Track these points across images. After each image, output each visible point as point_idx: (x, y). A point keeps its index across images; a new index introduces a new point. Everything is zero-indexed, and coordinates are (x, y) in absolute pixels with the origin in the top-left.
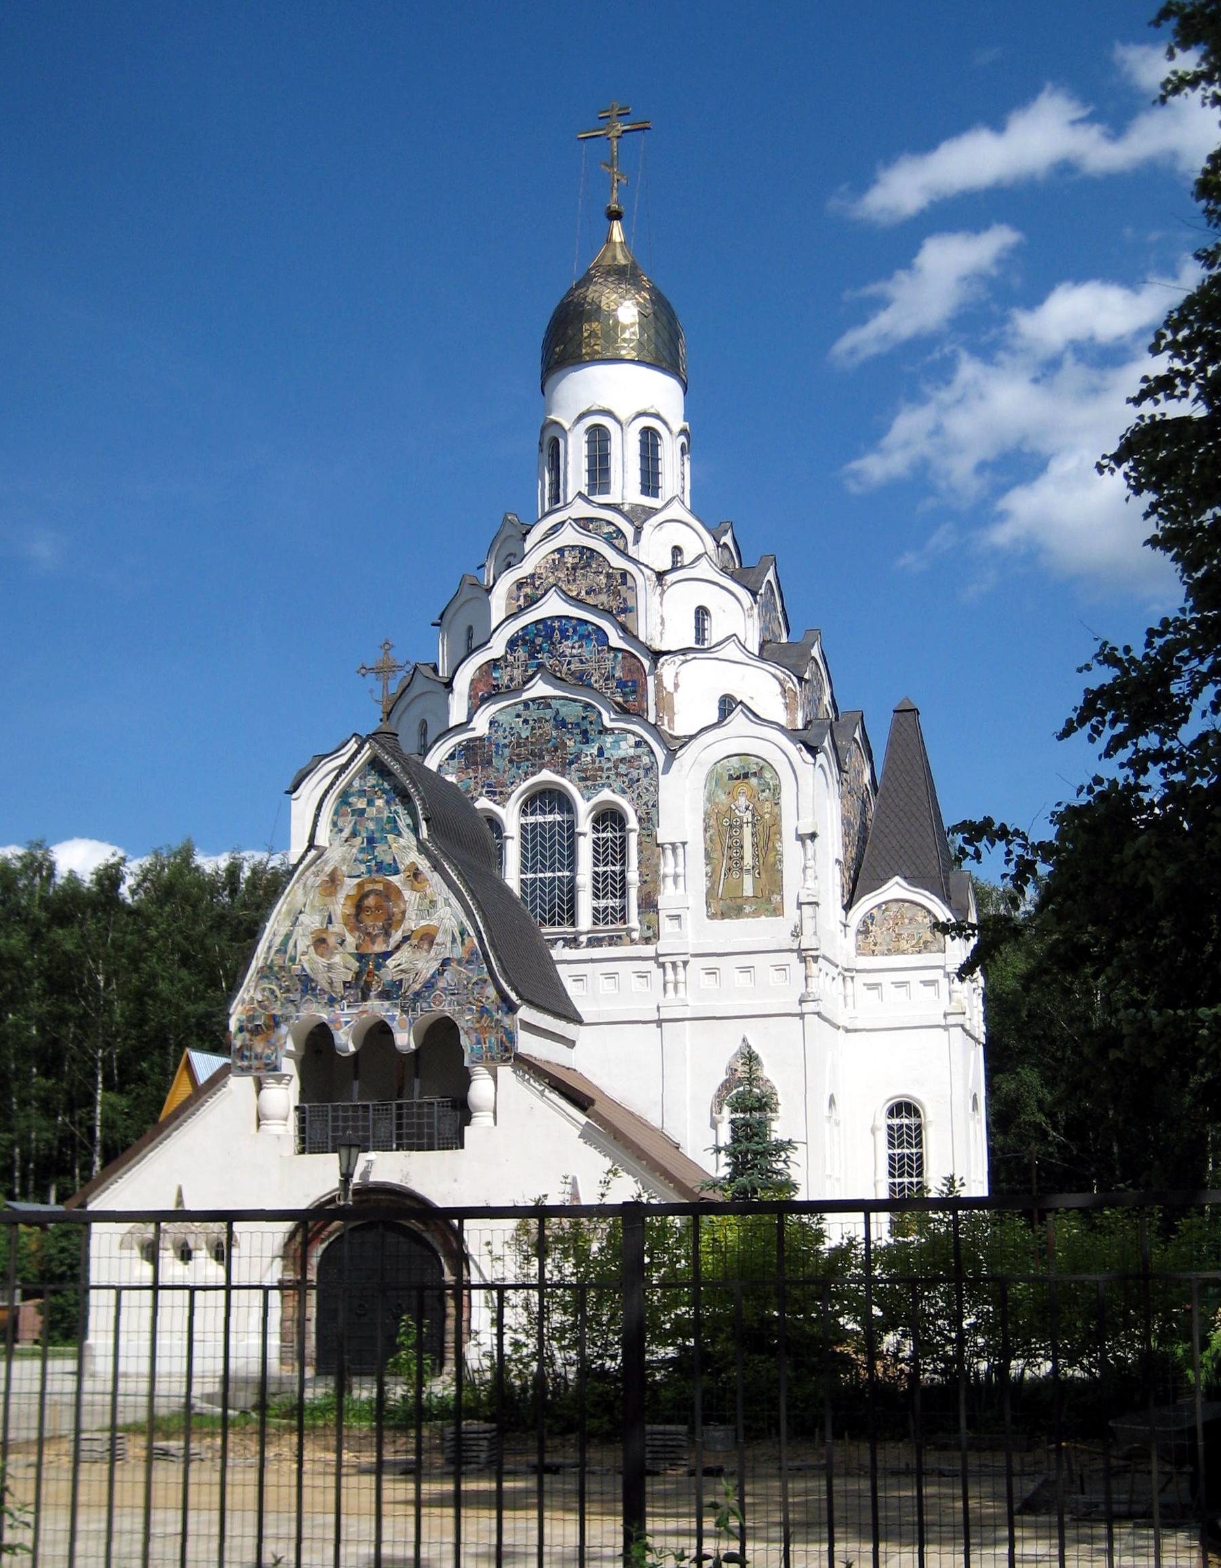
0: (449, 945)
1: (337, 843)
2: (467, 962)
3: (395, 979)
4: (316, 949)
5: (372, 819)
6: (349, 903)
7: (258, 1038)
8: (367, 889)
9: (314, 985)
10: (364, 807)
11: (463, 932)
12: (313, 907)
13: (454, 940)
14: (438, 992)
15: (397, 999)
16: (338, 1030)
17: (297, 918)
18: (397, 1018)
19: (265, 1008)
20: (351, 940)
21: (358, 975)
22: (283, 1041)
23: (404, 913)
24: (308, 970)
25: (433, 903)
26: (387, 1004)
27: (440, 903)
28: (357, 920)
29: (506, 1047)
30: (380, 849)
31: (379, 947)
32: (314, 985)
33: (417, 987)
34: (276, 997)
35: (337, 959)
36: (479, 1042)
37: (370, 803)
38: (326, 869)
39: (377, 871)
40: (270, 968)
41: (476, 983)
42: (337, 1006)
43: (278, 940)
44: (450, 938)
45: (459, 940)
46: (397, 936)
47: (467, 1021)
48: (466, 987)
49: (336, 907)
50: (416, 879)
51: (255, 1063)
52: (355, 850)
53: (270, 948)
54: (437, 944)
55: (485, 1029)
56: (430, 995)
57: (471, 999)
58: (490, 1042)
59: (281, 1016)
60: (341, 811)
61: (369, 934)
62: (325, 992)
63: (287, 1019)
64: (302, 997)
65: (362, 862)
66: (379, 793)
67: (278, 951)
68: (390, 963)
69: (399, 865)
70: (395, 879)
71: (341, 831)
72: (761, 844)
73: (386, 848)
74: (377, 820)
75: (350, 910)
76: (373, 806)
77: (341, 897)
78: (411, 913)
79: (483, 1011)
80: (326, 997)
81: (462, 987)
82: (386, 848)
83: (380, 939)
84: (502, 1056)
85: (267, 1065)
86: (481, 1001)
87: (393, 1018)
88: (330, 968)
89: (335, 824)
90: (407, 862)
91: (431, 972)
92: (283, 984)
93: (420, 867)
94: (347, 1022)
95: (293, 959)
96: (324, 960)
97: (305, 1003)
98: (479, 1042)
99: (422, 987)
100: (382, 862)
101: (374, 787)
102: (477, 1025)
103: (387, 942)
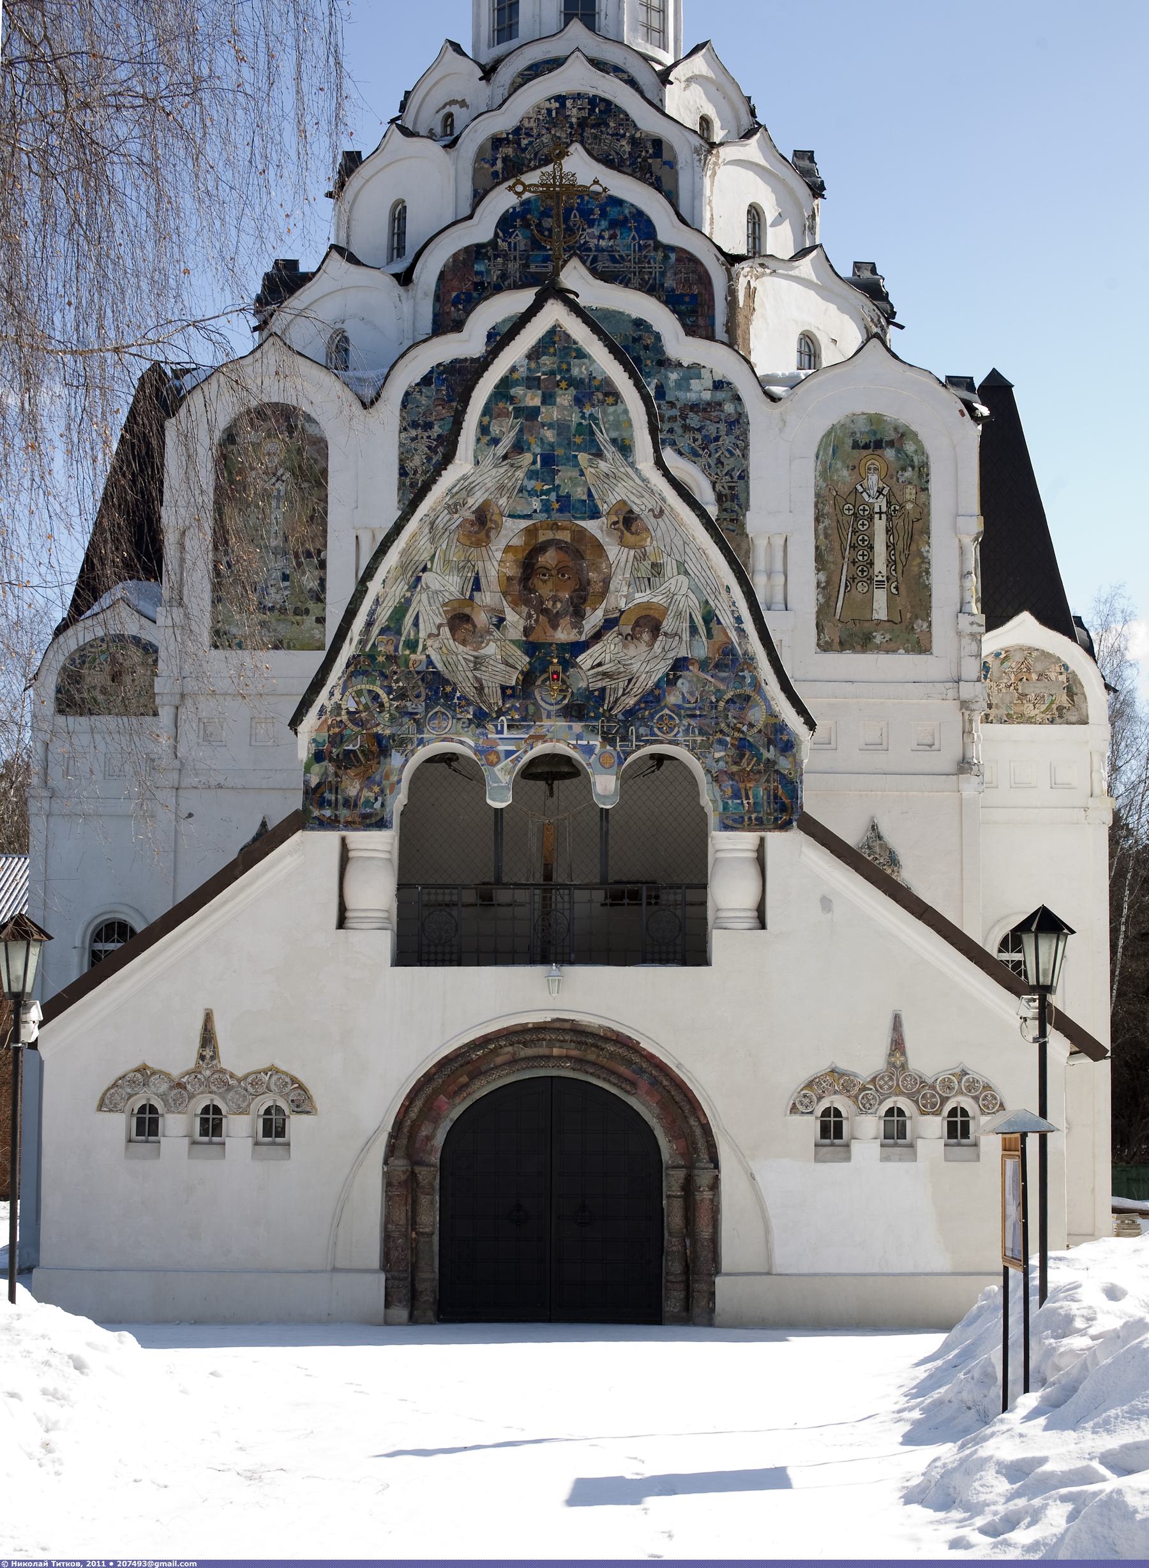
0: (686, 636)
1: (488, 462)
2: (717, 666)
4: (453, 630)
5: (551, 426)
6: (510, 556)
7: (351, 773)
8: (541, 539)
9: (449, 689)
10: (537, 402)
11: (710, 617)
12: (447, 562)
13: (694, 630)
14: (666, 711)
15: (596, 718)
16: (493, 765)
17: (419, 579)
19: (361, 724)
20: (514, 619)
21: (528, 678)
22: (394, 779)
23: (606, 582)
24: (440, 666)
25: (657, 569)
26: (578, 727)
27: (670, 568)
28: (525, 588)
29: (783, 804)
30: (565, 476)
31: (564, 634)
32: (449, 689)
33: (631, 701)
34: (382, 705)
35: (490, 649)
36: (736, 795)
37: (548, 399)
38: (471, 501)
39: (560, 510)
40: (372, 657)
41: (730, 701)
42: (490, 726)
43: (384, 616)
44: (686, 625)
45: (702, 629)
46: (594, 619)
47: (717, 761)
48: (714, 706)
49: (488, 565)
50: (628, 528)
51: (344, 813)
52: (520, 474)
53: (369, 624)
54: (666, 634)
55: (744, 776)
56: (652, 716)
58: (755, 796)
59: (392, 736)
60: (496, 411)
61: (545, 612)
64: (427, 711)
65: (533, 493)
66: (563, 384)
67: (382, 632)
68: (585, 660)
69: (599, 502)
70: (591, 526)
71: (495, 441)
72: (900, 546)
73: (576, 474)
74: (561, 427)
75: (512, 570)
76: (554, 404)
77: (497, 549)
78: (619, 583)
79: (743, 747)
80: (471, 710)
82: (576, 474)
83: (565, 621)
84: (776, 819)
86: (740, 731)
87: (589, 750)
88: (478, 663)
89: (484, 429)
90: (613, 499)
91: (655, 678)
93: (636, 509)
94: (509, 753)
95: (412, 645)
96: (467, 649)
97: (429, 721)
98: (736, 795)
99: (637, 703)
100: (568, 496)
101: (552, 373)
102: (735, 768)
103: (578, 625)
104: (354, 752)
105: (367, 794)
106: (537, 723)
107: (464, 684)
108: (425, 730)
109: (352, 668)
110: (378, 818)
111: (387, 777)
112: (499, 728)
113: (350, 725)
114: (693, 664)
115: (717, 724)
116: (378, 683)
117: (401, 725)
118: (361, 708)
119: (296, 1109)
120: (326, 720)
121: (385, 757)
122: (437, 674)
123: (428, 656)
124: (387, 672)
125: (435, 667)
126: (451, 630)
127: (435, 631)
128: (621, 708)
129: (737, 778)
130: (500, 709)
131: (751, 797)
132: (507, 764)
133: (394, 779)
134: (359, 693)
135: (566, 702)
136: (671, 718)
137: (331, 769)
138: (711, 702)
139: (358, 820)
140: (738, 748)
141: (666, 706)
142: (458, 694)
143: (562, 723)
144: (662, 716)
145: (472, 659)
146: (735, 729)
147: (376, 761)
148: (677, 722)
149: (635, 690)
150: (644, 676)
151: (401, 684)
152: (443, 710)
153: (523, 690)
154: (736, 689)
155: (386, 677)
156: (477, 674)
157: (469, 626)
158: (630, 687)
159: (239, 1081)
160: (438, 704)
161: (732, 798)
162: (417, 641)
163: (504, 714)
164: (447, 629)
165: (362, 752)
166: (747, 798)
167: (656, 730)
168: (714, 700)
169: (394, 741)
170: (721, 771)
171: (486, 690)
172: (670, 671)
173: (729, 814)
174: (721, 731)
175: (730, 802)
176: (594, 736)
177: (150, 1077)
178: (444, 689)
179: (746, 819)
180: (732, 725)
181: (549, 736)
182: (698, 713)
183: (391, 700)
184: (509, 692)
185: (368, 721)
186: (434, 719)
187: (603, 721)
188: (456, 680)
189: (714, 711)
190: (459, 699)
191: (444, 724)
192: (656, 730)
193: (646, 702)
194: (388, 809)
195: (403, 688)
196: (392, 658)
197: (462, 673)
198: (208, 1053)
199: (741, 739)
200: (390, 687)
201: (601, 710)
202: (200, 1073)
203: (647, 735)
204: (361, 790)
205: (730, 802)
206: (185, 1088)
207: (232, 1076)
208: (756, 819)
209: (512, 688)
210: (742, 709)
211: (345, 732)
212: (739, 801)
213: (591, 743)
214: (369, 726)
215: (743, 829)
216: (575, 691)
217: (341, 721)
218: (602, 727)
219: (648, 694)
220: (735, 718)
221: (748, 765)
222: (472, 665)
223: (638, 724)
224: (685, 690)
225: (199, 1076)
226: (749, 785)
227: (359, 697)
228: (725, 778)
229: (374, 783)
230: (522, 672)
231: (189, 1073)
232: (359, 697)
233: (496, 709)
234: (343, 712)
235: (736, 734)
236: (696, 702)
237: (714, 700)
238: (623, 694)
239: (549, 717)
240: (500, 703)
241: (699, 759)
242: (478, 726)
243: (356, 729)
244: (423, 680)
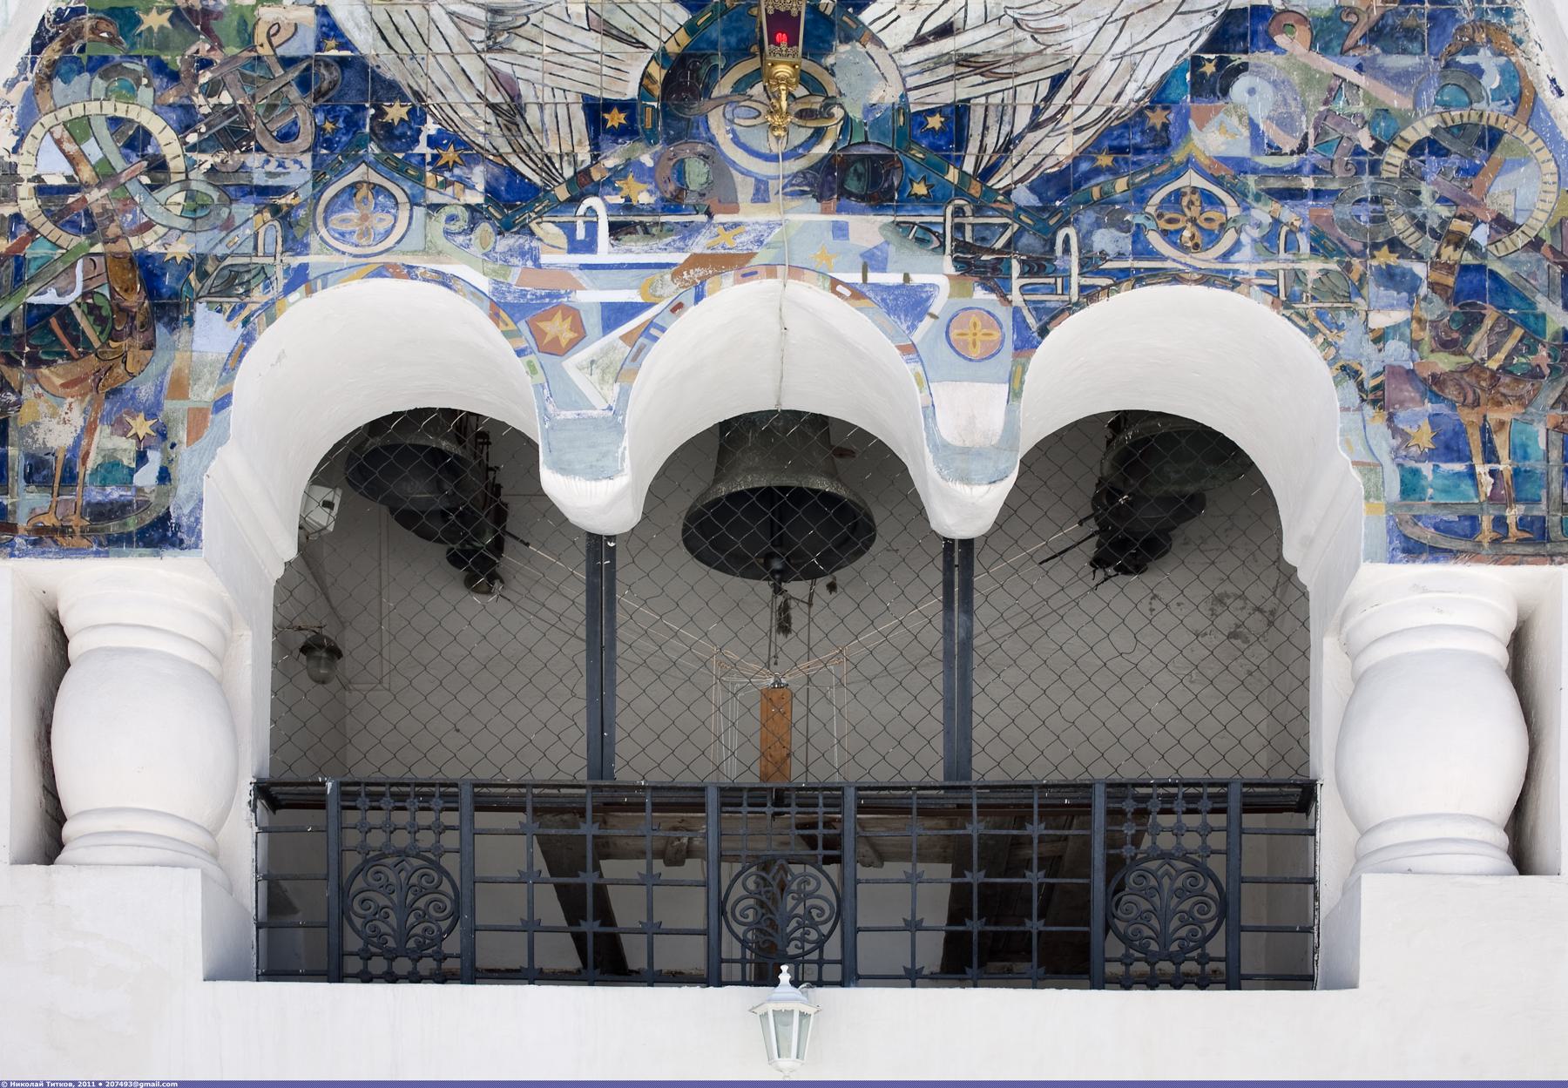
3: (916, 104)
7: (53, 376)
14: (1191, 179)
15: (934, 201)
18: (937, 306)
19: (90, 225)
22: (204, 394)
24: (365, 41)
26: (868, 228)
33: (1062, 147)
34: (158, 166)
36: (1450, 446)
42: (548, 230)
47: (1380, 338)
56: (1139, 196)
57: (1400, 225)
58: (1520, 451)
59: (197, 263)
62: (470, 154)
64: (319, 179)
80: (478, 176)
81: (1342, 157)
85: (102, 513)
86: (1460, 241)
91: (1150, 73)
92: (203, 105)
94: (615, 315)
98: (1450, 446)
99: (1085, 154)
102: (1444, 363)
104: (63, 312)
105: (109, 442)
106: (719, 218)
107: (452, 97)
108: (314, 240)
109: (52, 52)
110: (149, 518)
111: (179, 388)
112: (581, 234)
113: (48, 228)
114: (1287, 29)
115: (1379, 220)
116: (146, 94)
117: (228, 226)
118: (86, 174)
121: (173, 325)
122: (353, 66)
124: (176, 61)
125: (345, 44)
128: (1024, 168)
129: (1451, 392)
131: (1503, 453)
133: (204, 394)
134: (79, 129)
135: (823, 149)
136: (1209, 199)
138: (1358, 151)
139: (76, 521)
140: (1454, 296)
141: (1189, 163)
142: (431, 128)
143: (809, 217)
144: (1178, 194)
145: (481, 15)
146: (1443, 234)
147: (139, 340)
148: (1233, 210)
149: (1077, 110)
150: (1108, 67)
151: (226, 98)
152: (375, 178)
153: (666, 113)
154: (1447, 106)
155: (174, 77)
156: (500, 62)
158: (1060, 99)
160: (358, 161)
161: (1430, 456)
163: (596, 189)
165: (93, 310)
166: (1490, 455)
167: (1155, 240)
168: (1366, 143)
169: (203, 275)
170: (1393, 371)
171: (532, 115)
172: (1206, 48)
173: (1423, 508)
174: (1394, 244)
175: (1426, 468)
176: (924, 257)
178: (381, 113)
179: (1486, 522)
180: (1433, 222)
181: (763, 256)
182: (1308, 183)
183: (193, 148)
184: (615, 119)
185: (110, 216)
186: (344, 206)
187: (959, 212)
188: (422, 85)
189: (1367, 179)
190: (432, 142)
191: (381, 222)
192: (1155, 240)
193: (1117, 150)
194: (183, 490)
195: (233, 110)
197: (446, 62)
199: (1466, 269)
200: (188, 109)
201: (952, 175)
203: (1120, 256)
204: (89, 429)
205: (1426, 468)
208: (1522, 523)
209: (625, 106)
210: (1471, 172)
211: (29, 252)
212: (1460, 467)
213: (917, 279)
214: (113, 230)
215: (1474, 556)
216: (857, 115)
217: (17, 217)
218: (959, 228)
219: (1125, 126)
220: (1442, 200)
221: (1492, 352)
222: (479, 35)
223: (1088, 217)
224: (1260, 112)
226: (1494, 416)
228: (1409, 392)
229: (135, 407)
230: (662, 57)
232: (75, 140)
233: (569, 172)
234: (25, 190)
235: (1449, 254)
236: (1302, 149)
237: (1366, 143)
238: (1034, 126)
239: (761, 194)
240: (584, 155)
241: (1312, 332)
242: (504, 228)
243: (69, 240)
244: (304, 83)
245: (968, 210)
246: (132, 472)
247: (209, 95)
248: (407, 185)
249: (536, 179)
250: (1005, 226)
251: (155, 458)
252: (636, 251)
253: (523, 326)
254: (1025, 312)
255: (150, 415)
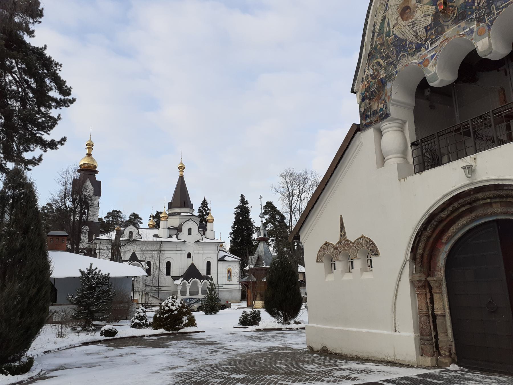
15: (472, 14)
16: (426, 66)
17: (387, 5)
22: (389, 94)
26: (463, 24)
34: (381, 66)
35: (418, 14)
40: (376, 48)
51: (374, 118)
63: (391, 76)
87: (472, 31)
88: (413, 24)
94: (432, 57)
97: (399, 60)
104: (374, 90)
105: (381, 106)
106: (443, 34)
111: (386, 94)
112: (427, 47)
118: (375, 71)
119: (372, 254)
120: (364, 84)
123: (395, 34)
125: (398, 37)
126: (401, 17)
127: (396, 22)
130: (426, 38)
132: (433, 62)
135: (455, 16)
137: (367, 101)
142: (408, 43)
152: (403, 54)
156: (414, 29)
157: (409, 10)
159: (353, 243)
162: (390, 30)
164: (400, 18)
169: (387, 78)
177: (328, 246)
184: (429, 28)
187: (476, 13)
196: (382, 44)
198: (343, 233)
201: (474, 7)
202: (341, 242)
206: (338, 249)
207: (351, 242)
209: (429, 26)
213: (471, 27)
218: (476, 15)
225: (341, 243)
227: (373, 67)
230: (433, 15)
231: (338, 243)
234: (369, 77)
239: (448, 28)
240: (426, 36)
244: (394, 46)
245: (477, 12)
246: (383, 109)
247: (384, 53)
248: (406, 52)
249: (421, 42)
250: (483, 11)
251: (385, 106)
252: (434, 46)
253: (422, 65)
254: (489, 23)
255: (384, 100)
